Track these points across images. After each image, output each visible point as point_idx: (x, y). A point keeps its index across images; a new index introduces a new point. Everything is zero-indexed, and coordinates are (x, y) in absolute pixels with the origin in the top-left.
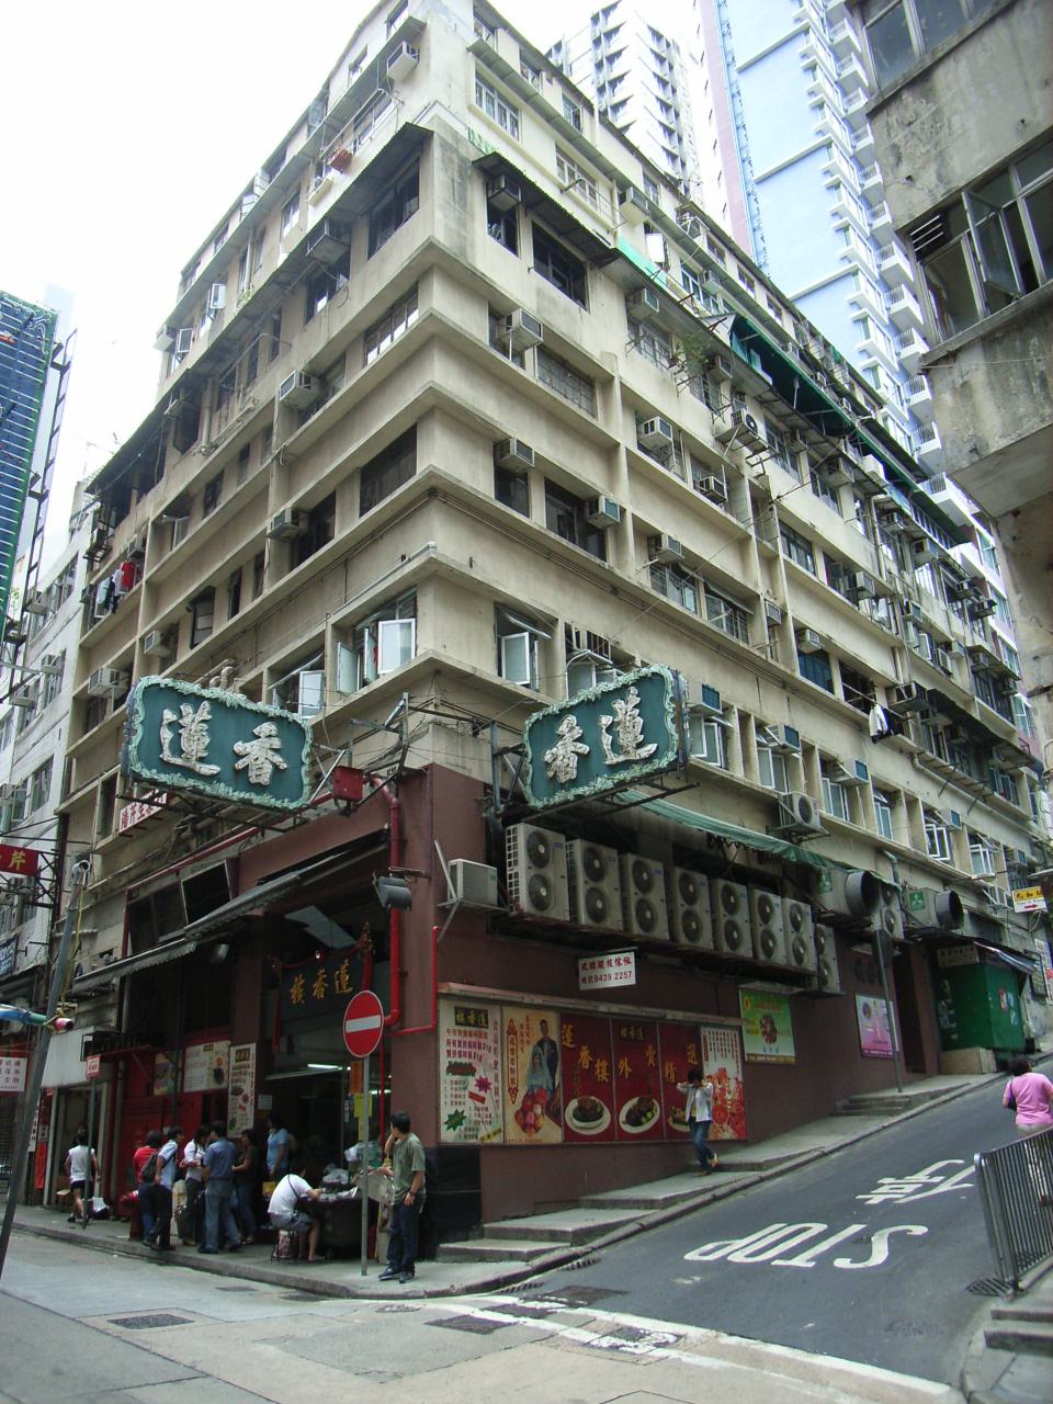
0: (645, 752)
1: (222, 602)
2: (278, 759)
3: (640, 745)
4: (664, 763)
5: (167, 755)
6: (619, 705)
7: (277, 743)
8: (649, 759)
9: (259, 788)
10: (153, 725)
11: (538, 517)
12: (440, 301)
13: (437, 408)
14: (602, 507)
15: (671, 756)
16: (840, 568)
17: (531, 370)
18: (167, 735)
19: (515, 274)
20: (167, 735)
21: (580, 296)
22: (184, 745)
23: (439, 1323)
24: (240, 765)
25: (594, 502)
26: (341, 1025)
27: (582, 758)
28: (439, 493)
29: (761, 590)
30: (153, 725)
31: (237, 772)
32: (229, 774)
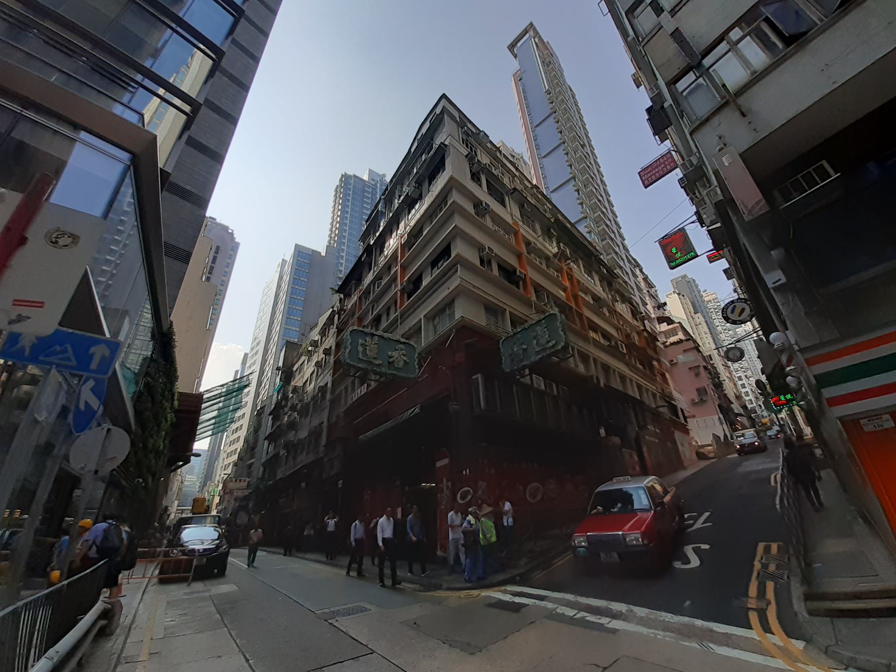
0: (550, 344)
1: (384, 318)
2: (405, 358)
3: (548, 342)
4: (560, 347)
5: (361, 356)
6: (538, 328)
7: (404, 352)
8: (553, 346)
9: (398, 369)
10: (354, 345)
11: (496, 271)
12: (455, 197)
13: (457, 233)
14: (518, 273)
15: (563, 344)
16: (596, 298)
17: (489, 222)
18: (360, 349)
19: (482, 193)
20: (360, 349)
21: (503, 203)
22: (368, 352)
23: (491, 605)
24: (391, 360)
25: (515, 272)
26: (435, 465)
27: (524, 350)
28: (460, 261)
29: (573, 305)
30: (354, 345)
31: (389, 363)
32: (386, 363)
